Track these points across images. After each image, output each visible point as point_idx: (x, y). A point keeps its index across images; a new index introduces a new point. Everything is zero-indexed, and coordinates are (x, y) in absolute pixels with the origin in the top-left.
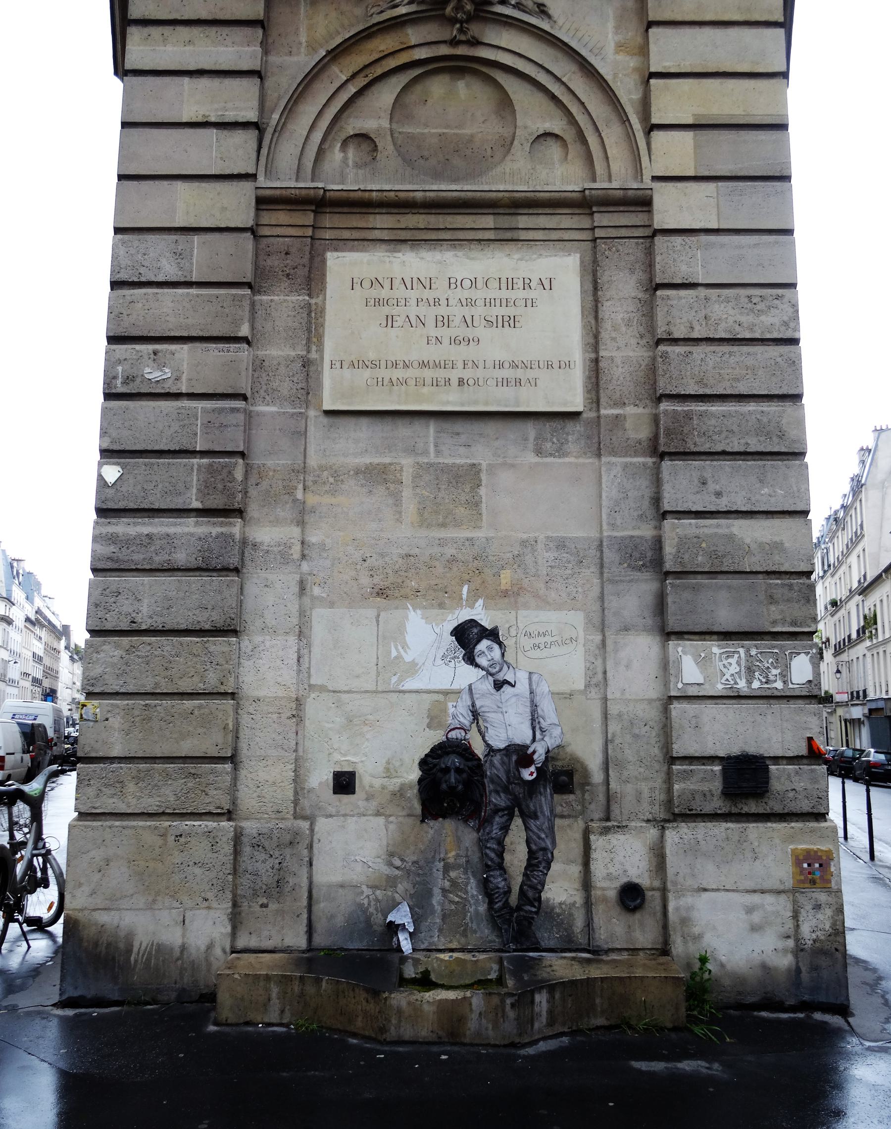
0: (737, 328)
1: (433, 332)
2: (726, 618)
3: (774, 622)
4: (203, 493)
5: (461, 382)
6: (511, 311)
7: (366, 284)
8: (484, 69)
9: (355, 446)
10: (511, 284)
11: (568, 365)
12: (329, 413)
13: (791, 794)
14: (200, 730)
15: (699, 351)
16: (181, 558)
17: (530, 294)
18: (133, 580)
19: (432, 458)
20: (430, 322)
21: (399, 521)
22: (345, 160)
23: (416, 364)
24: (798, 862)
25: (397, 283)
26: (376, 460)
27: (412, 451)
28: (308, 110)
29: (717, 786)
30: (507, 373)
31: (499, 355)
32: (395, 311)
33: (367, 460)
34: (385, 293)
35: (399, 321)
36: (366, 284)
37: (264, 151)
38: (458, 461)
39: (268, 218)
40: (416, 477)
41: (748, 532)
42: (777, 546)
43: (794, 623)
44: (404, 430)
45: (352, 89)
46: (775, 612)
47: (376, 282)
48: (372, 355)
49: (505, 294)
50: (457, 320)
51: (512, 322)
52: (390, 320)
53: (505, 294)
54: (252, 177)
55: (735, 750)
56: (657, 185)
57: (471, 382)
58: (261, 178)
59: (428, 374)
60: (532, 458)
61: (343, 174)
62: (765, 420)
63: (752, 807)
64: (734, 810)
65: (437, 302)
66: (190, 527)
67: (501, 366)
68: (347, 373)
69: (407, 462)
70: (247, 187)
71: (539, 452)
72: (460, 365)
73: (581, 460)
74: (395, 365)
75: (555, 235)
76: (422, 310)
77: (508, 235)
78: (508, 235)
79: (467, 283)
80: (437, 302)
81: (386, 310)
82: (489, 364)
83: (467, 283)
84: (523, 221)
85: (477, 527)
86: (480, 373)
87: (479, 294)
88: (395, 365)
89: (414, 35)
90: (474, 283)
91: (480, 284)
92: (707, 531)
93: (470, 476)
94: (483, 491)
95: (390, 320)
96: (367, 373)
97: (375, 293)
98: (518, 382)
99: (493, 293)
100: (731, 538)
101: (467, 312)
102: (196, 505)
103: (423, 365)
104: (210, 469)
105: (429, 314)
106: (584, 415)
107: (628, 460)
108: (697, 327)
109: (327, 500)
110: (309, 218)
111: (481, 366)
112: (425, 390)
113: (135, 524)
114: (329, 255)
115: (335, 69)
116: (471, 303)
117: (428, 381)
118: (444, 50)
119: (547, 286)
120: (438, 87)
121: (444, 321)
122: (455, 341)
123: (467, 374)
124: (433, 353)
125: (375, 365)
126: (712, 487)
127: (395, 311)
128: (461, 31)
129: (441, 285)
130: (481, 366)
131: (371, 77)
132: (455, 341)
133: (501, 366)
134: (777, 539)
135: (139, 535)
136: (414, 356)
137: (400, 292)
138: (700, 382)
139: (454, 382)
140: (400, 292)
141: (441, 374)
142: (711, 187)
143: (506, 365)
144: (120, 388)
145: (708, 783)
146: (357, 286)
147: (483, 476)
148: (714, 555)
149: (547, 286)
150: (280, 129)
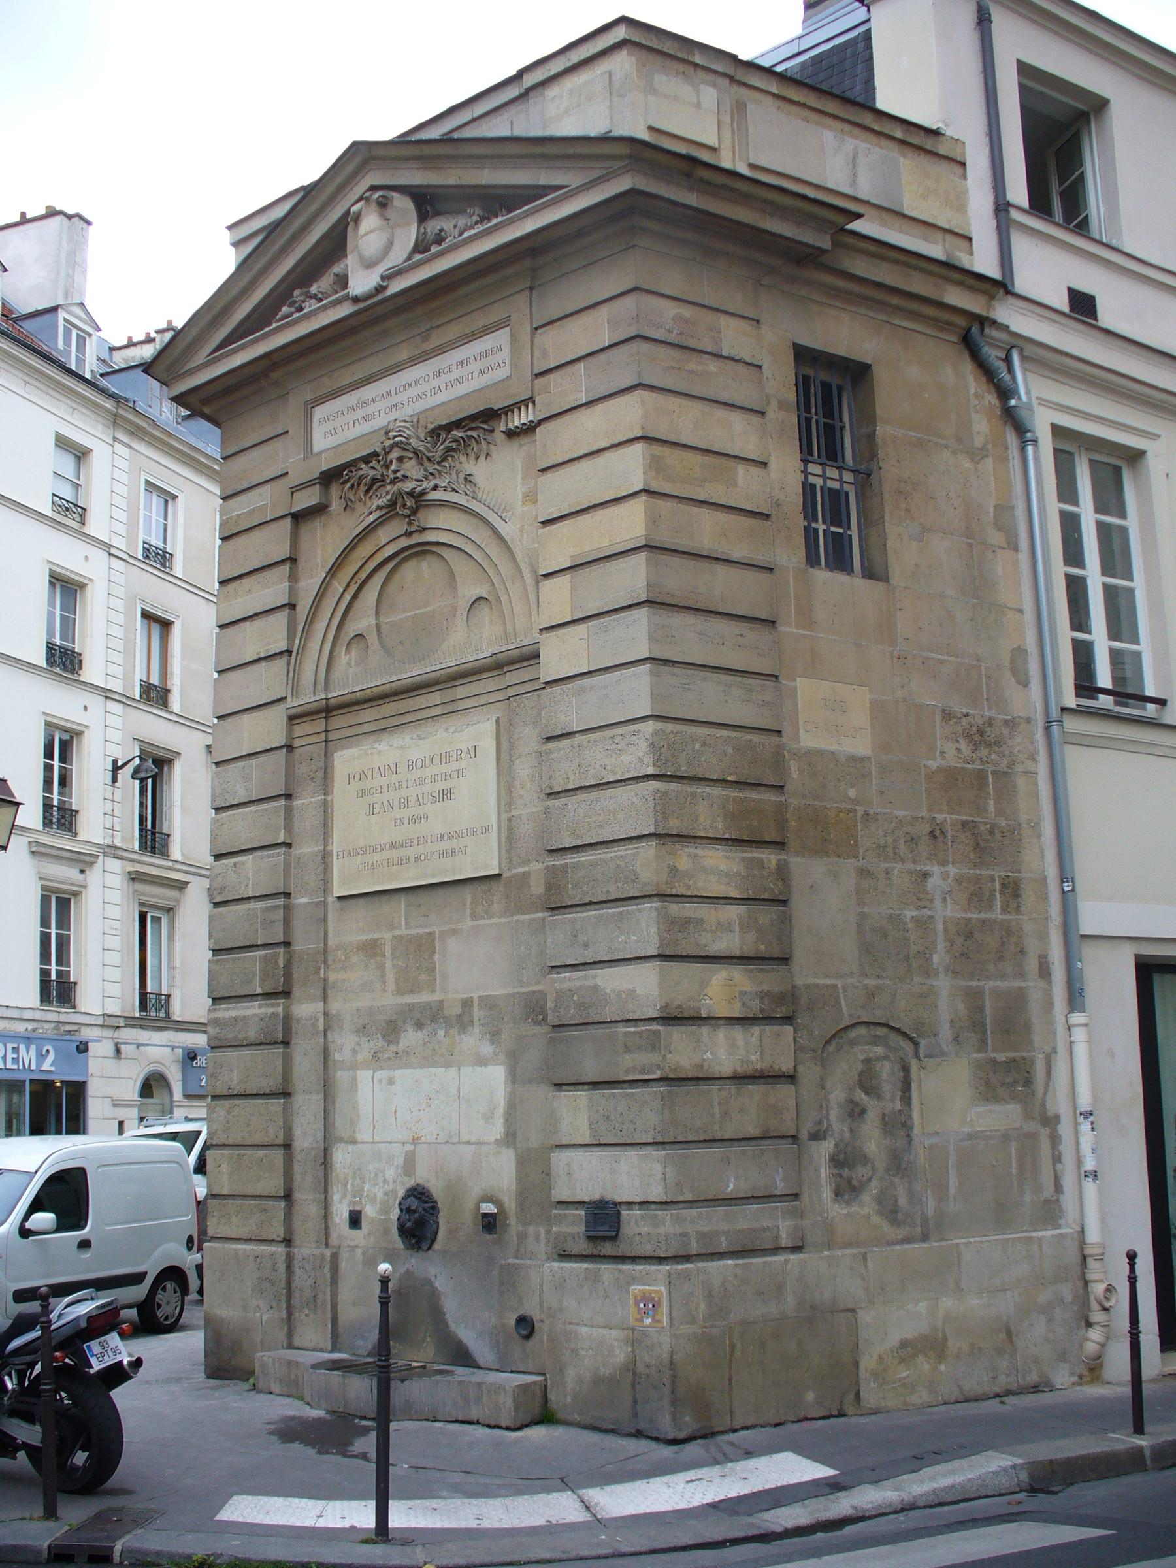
0: (604, 773)
2: (591, 1069)
3: (627, 1071)
4: (263, 982)
8: (434, 549)
9: (348, 930)
10: (447, 758)
12: (339, 898)
13: (637, 1238)
14: (267, 1175)
15: (573, 801)
16: (252, 1034)
18: (230, 1054)
19: (403, 931)
21: (384, 991)
22: (349, 664)
24: (637, 1303)
26: (369, 937)
27: (391, 926)
28: (320, 626)
29: (582, 1228)
30: (446, 845)
33: (364, 937)
34: (369, 784)
37: (291, 674)
38: (421, 931)
39: (299, 730)
40: (394, 949)
41: (611, 980)
42: (631, 993)
43: (643, 1071)
44: (386, 907)
45: (348, 597)
46: (628, 1060)
47: (363, 775)
48: (361, 843)
51: (448, 794)
52: (372, 806)
54: (283, 699)
55: (597, 1197)
56: (546, 635)
58: (289, 699)
59: (395, 854)
60: (470, 923)
61: (353, 675)
62: (622, 864)
63: (607, 1249)
64: (596, 1252)
66: (254, 1009)
69: (388, 936)
70: (281, 707)
71: (473, 916)
73: (503, 920)
75: (482, 700)
77: (450, 708)
78: (450, 708)
81: (369, 799)
84: (461, 692)
85: (433, 991)
89: (384, 535)
92: (577, 983)
93: (422, 948)
94: (437, 957)
98: (454, 852)
100: (596, 988)
102: (259, 991)
103: (393, 846)
104: (265, 960)
106: (504, 875)
107: (533, 916)
108: (572, 778)
109: (342, 975)
110: (320, 725)
113: (228, 1009)
115: (335, 583)
118: (404, 542)
120: (409, 571)
121: (405, 803)
124: (396, 834)
125: (362, 851)
126: (582, 938)
128: (410, 523)
129: (402, 768)
131: (359, 582)
134: (631, 987)
135: (231, 1018)
136: (386, 840)
137: (380, 781)
138: (575, 834)
142: (581, 628)
144: (218, 899)
145: (574, 1226)
147: (437, 943)
148: (581, 1006)
150: (303, 648)
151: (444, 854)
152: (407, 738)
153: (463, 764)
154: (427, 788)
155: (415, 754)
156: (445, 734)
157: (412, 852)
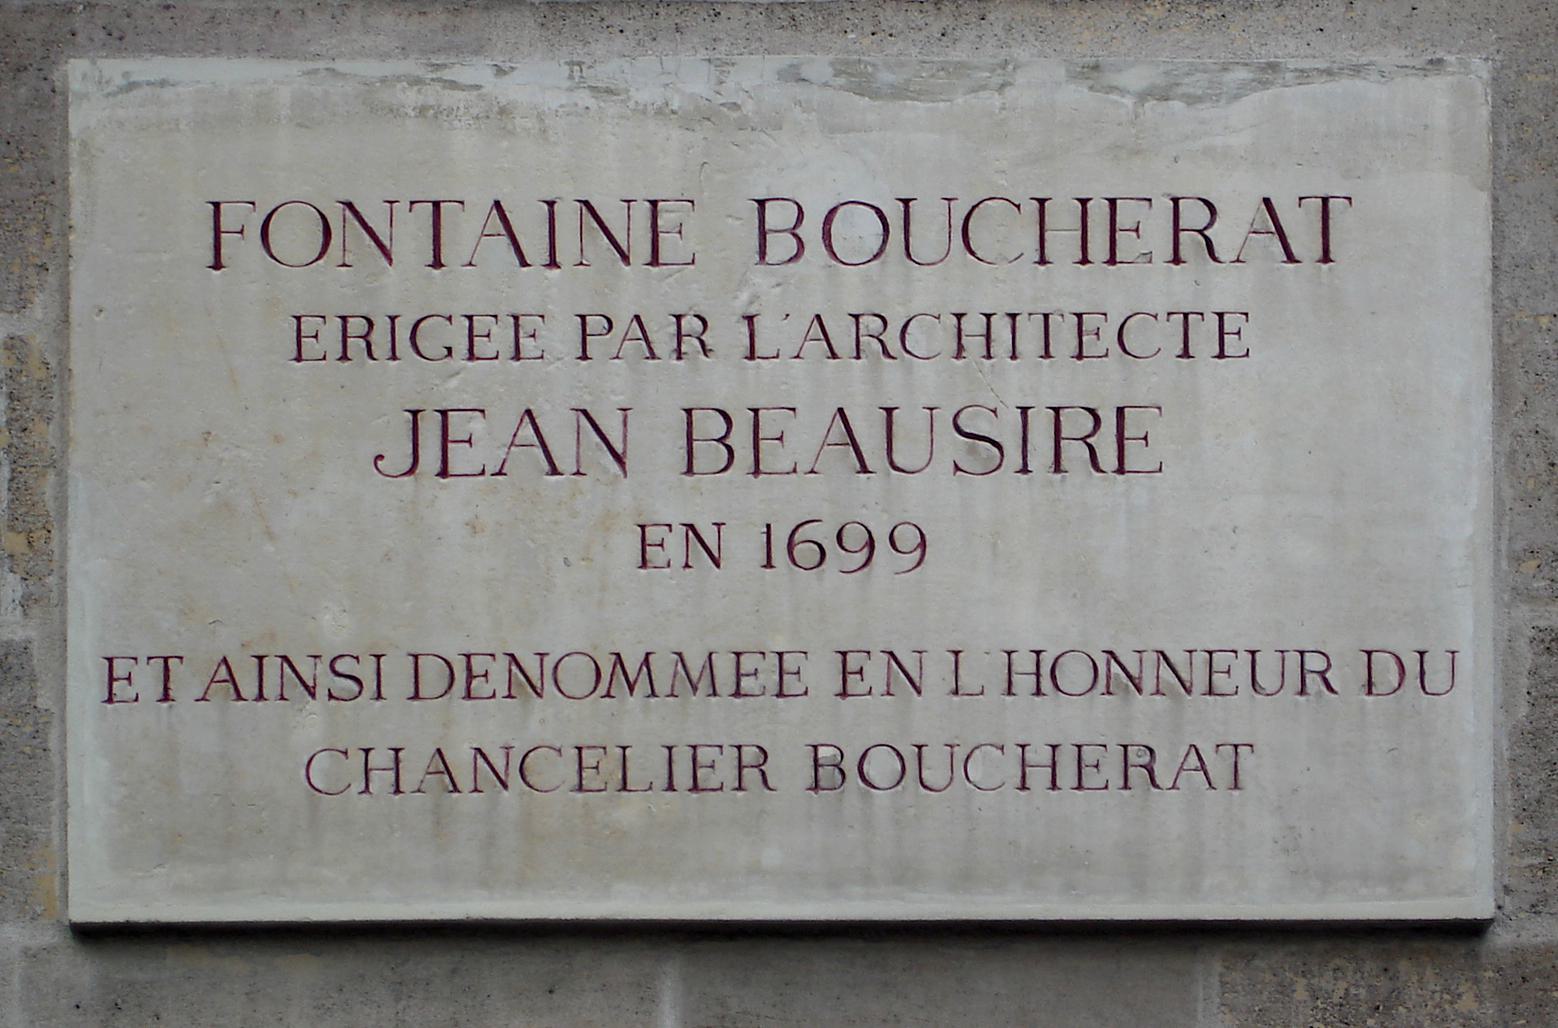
1: (674, 502)
5: (826, 773)
6: (1102, 383)
7: (296, 236)
10: (1102, 233)
11: (1415, 671)
12: (92, 936)
17: (1224, 288)
20: (656, 445)
23: (577, 674)
25: (464, 229)
30: (1077, 718)
31: (1032, 623)
32: (458, 383)
34: (400, 287)
35: (484, 441)
36: (296, 236)
47: (342, 227)
49: (1067, 286)
50: (806, 434)
51: (1111, 440)
53: (1067, 286)
57: (881, 767)
59: (644, 725)
65: (690, 335)
67: (1047, 676)
68: (196, 722)
72: (821, 674)
74: (463, 678)
76: (611, 382)
79: (858, 231)
80: (690, 335)
81: (405, 380)
82: (983, 670)
83: (858, 231)
86: (930, 718)
87: (927, 290)
88: (463, 678)
90: (897, 225)
91: (929, 234)
95: (431, 441)
96: (311, 723)
97: (335, 287)
98: (1139, 767)
99: (1006, 283)
101: (857, 387)
103: (618, 676)
105: (652, 396)
111: (936, 675)
112: (629, 810)
114: (77, 72)
116: (880, 338)
117: (647, 765)
119: (1305, 242)
121: (739, 441)
122: (791, 548)
123: (862, 724)
124: (664, 613)
125: (352, 678)
127: (458, 383)
129: (713, 235)
130: (936, 675)
132: (791, 548)
133: (1047, 676)
136: (565, 630)
137: (482, 279)
139: (790, 769)
140: (482, 279)
141: (716, 722)
143: (1075, 674)
146: (243, 250)
149: (1305, 242)
151: (1068, 768)
152: (755, 76)
153: (1224, 288)
154: (925, 382)
155: (815, 170)
156: (1076, 96)
157: (787, 731)
